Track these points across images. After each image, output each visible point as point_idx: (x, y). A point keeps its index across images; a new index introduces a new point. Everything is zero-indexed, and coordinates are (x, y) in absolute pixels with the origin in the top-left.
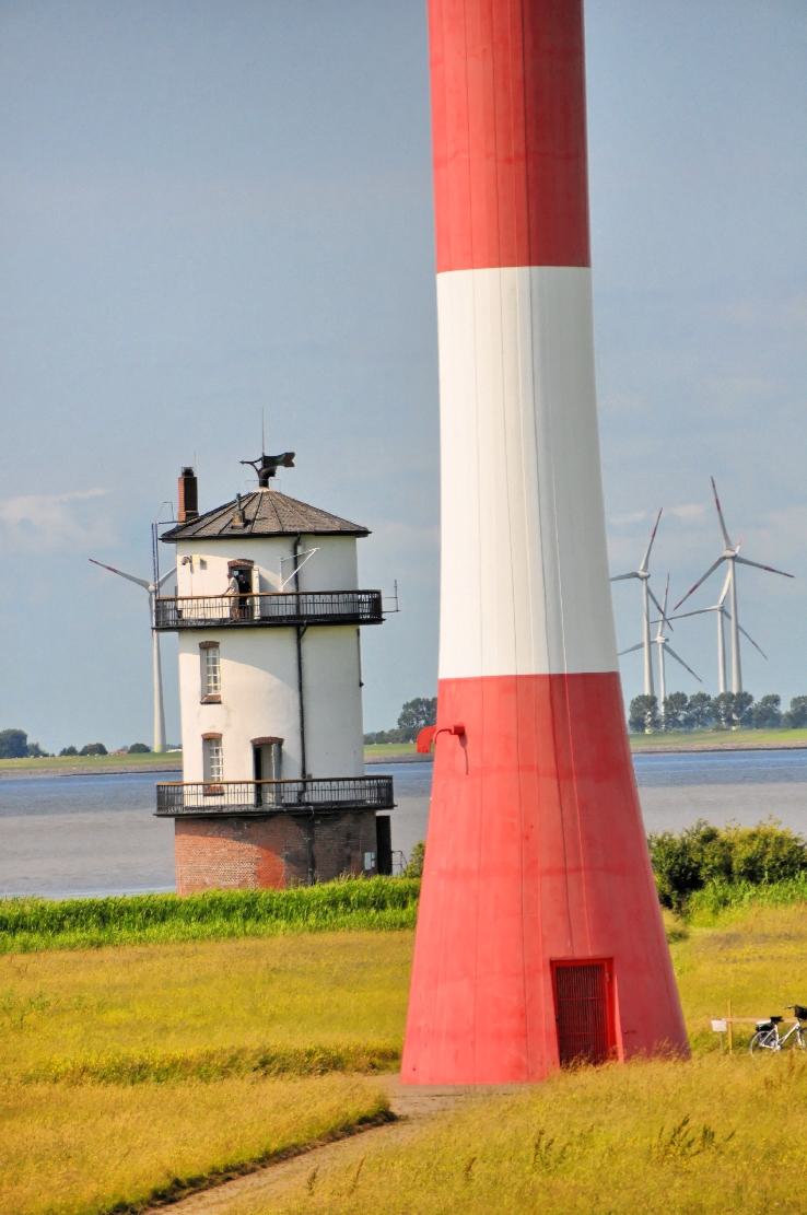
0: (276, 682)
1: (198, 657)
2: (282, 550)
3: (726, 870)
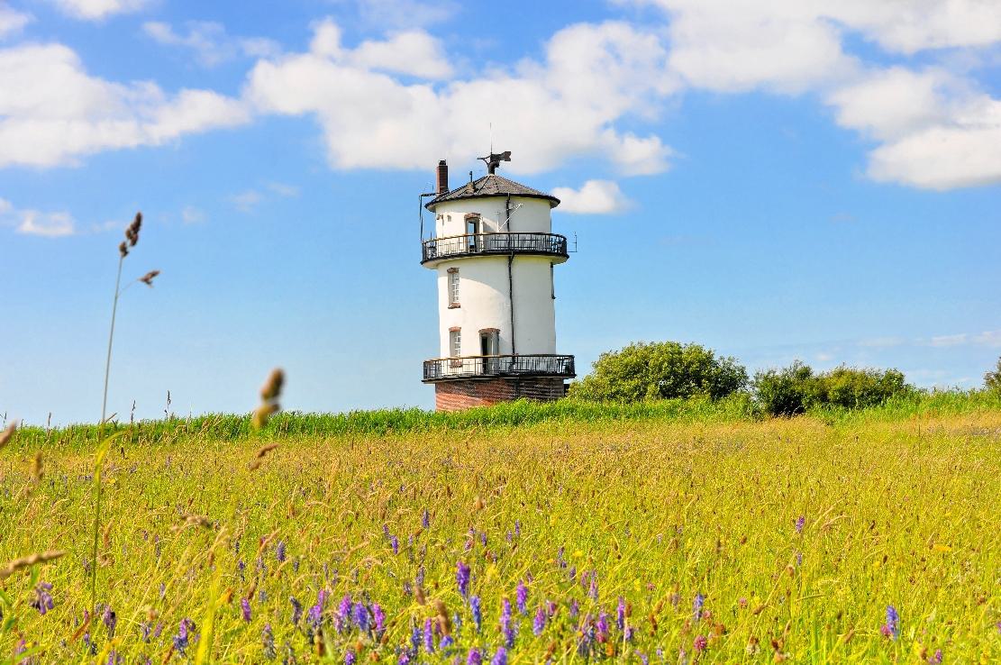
0: (495, 291)
1: (447, 278)
2: (499, 205)
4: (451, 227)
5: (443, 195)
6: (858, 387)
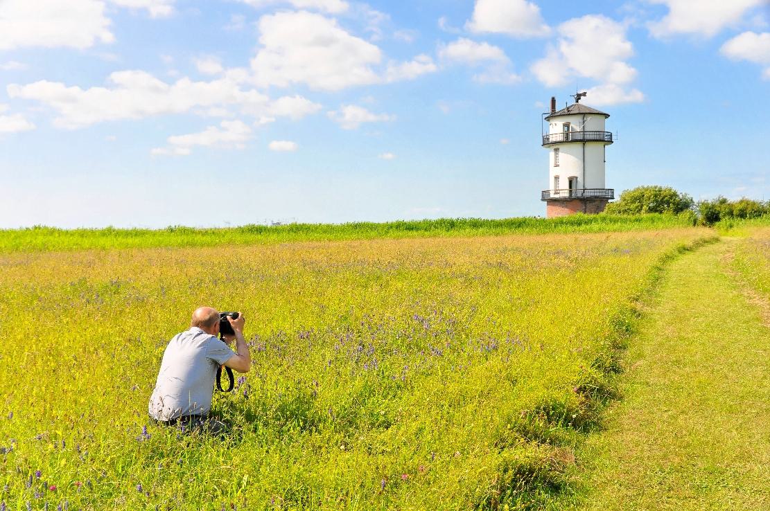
2: (579, 118)
3: (731, 213)
4: (556, 129)
5: (553, 115)
6: (749, 209)
